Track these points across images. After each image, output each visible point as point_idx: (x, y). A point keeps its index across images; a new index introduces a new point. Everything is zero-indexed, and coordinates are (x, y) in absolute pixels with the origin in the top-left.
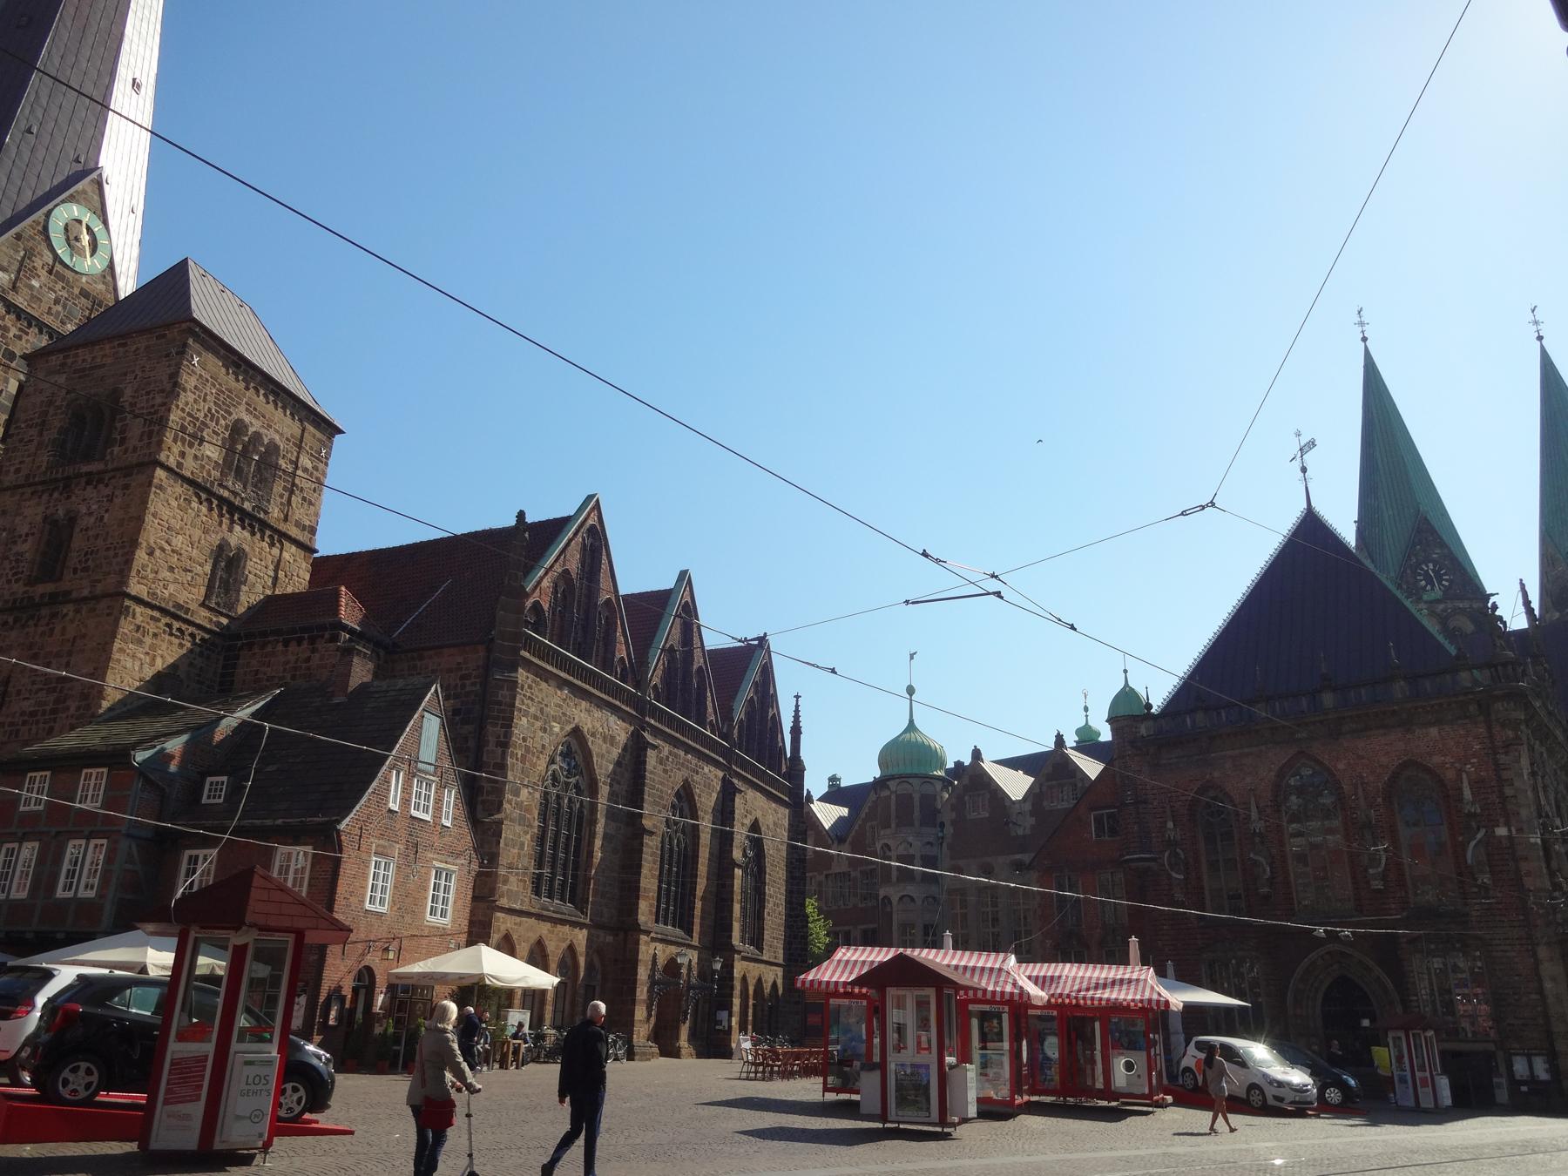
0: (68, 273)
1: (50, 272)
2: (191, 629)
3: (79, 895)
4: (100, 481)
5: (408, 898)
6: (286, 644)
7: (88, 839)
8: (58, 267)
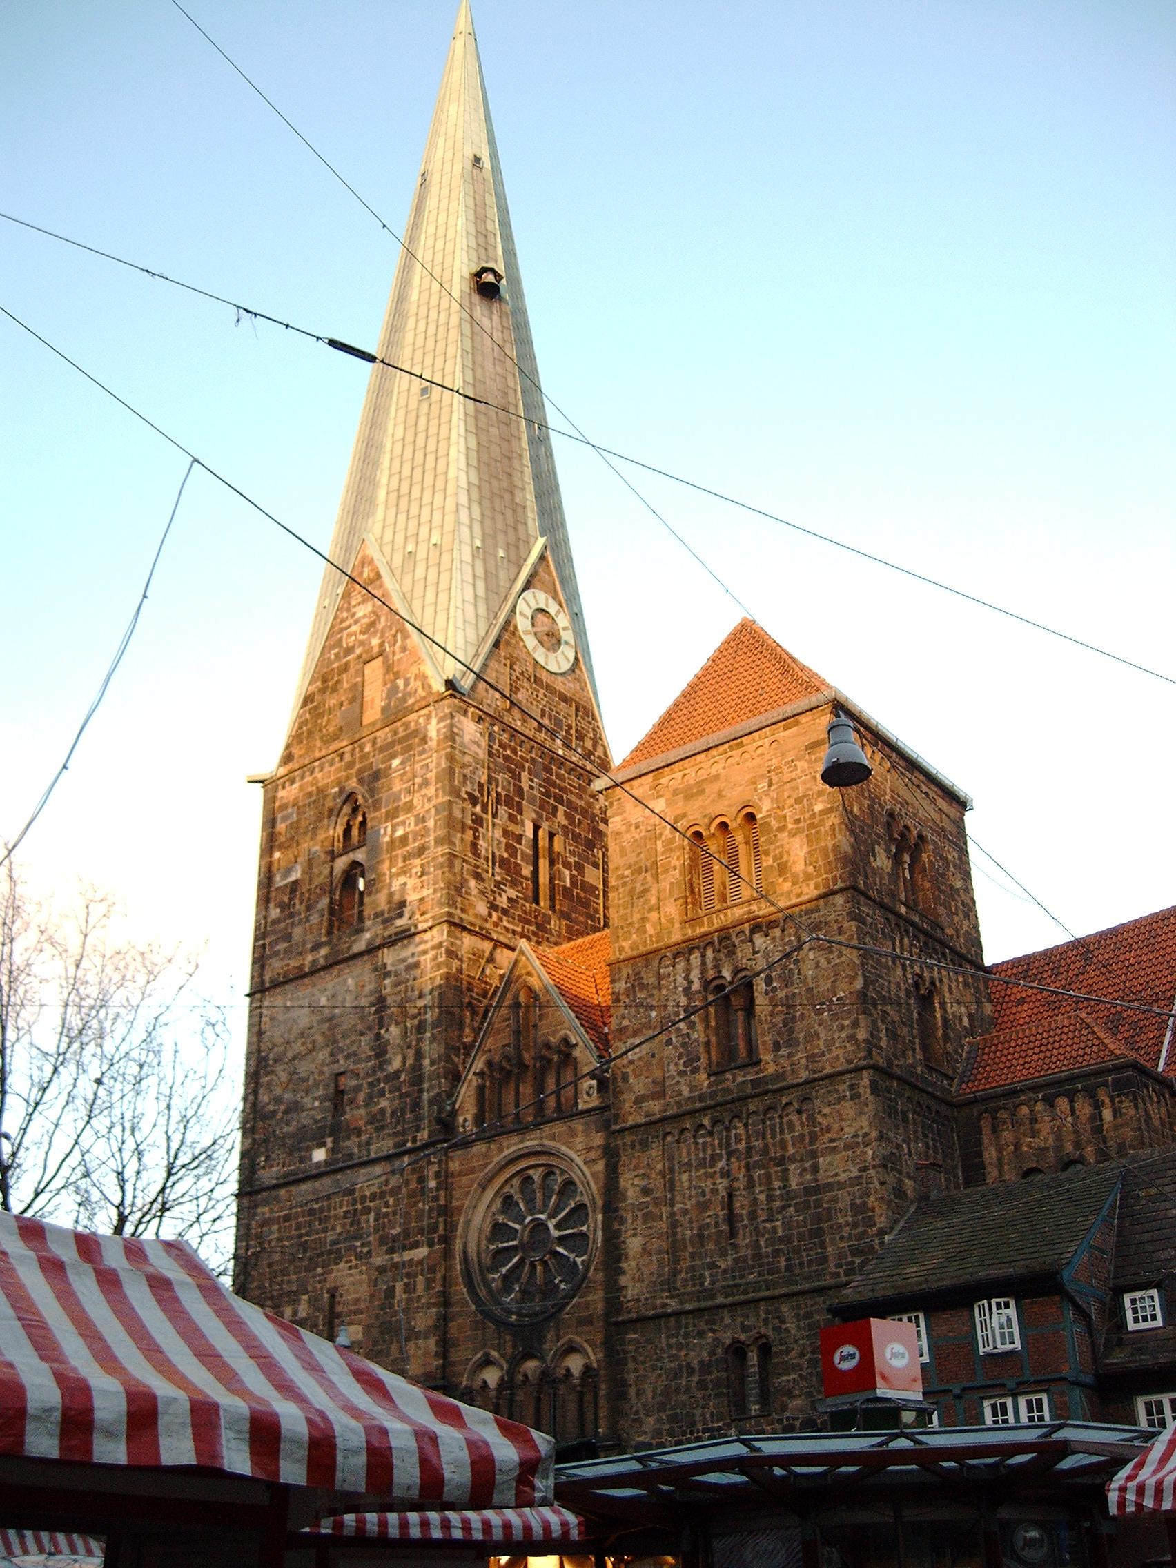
0: (544, 676)
1: (529, 680)
7: (1015, 1396)
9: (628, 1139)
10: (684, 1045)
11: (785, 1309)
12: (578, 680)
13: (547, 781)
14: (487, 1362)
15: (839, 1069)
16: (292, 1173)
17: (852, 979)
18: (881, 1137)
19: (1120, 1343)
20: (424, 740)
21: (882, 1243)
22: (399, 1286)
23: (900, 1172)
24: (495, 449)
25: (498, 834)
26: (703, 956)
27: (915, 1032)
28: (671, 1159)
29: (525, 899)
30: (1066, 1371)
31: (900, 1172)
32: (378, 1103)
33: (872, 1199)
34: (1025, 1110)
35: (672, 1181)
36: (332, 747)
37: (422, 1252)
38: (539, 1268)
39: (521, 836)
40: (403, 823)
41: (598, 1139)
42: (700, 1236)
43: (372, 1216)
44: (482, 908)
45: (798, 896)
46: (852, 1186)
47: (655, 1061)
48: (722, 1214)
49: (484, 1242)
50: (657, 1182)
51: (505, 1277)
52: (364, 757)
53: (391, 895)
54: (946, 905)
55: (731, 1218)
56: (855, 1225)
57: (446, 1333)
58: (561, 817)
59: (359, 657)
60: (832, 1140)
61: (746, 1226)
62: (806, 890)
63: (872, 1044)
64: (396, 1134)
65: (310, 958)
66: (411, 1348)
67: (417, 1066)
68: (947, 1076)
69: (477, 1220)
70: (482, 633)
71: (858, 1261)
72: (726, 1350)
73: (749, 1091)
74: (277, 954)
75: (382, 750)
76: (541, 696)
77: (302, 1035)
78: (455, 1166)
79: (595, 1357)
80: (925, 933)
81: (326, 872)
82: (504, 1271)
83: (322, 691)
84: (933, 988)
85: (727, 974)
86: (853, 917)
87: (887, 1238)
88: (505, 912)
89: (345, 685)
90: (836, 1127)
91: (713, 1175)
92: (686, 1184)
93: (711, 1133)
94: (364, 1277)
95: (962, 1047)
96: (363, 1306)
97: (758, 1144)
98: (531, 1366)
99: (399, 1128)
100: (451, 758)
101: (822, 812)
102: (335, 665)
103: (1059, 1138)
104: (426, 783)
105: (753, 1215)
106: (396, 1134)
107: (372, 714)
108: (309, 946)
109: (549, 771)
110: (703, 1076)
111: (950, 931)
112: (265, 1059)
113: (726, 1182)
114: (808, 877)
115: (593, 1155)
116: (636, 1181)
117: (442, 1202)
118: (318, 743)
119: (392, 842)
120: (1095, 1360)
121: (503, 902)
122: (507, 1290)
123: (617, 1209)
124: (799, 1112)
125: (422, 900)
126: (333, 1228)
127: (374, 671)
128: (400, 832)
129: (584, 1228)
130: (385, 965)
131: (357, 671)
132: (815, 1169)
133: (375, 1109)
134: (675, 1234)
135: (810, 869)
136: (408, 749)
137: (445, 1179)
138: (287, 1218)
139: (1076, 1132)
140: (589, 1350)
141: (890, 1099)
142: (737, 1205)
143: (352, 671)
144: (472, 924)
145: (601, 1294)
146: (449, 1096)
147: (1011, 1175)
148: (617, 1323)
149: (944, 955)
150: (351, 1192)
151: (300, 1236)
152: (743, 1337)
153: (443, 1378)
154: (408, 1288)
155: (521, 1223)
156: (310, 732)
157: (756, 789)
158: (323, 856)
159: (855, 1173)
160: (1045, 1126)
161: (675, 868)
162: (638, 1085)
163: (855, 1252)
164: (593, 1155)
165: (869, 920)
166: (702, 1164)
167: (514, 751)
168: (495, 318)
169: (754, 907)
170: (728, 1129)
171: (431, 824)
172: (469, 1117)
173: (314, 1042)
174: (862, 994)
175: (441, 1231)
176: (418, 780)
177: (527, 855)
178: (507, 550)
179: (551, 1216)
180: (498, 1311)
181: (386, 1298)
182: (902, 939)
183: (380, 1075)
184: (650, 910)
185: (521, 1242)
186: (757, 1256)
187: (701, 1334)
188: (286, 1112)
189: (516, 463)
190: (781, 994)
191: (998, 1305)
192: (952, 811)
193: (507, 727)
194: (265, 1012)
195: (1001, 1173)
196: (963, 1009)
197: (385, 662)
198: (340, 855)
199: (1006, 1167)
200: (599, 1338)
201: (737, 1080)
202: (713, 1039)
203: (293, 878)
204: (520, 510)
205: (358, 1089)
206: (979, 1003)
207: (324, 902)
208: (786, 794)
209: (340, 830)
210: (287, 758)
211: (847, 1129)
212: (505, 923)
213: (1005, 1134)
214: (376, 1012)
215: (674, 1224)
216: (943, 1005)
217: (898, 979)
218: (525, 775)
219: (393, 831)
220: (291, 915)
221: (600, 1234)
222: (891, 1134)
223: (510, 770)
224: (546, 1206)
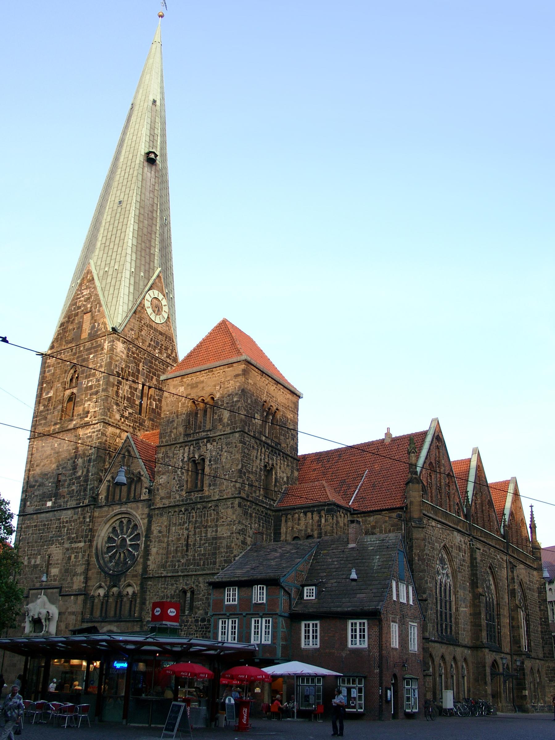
0: (153, 325)
1: (147, 326)
3: (263, 643)
4: (214, 441)
9: (157, 512)
10: (179, 480)
11: (201, 579)
12: (168, 326)
13: (150, 367)
14: (100, 587)
15: (229, 497)
16: (38, 509)
17: (237, 465)
18: (239, 522)
19: (301, 603)
21: (234, 560)
22: (73, 556)
23: (246, 535)
24: (145, 230)
25: (127, 388)
26: (189, 448)
27: (261, 484)
28: (170, 521)
29: (136, 413)
30: (278, 612)
31: (246, 535)
32: (72, 487)
33: (233, 544)
34: (297, 515)
35: (169, 529)
36: (70, 346)
37: (82, 545)
38: (122, 555)
39: (137, 388)
40: (91, 380)
41: (146, 511)
42: (176, 550)
43: (66, 529)
44: (118, 417)
45: (224, 431)
46: (227, 539)
47: (168, 485)
48: (185, 543)
49: (104, 543)
50: (164, 529)
51: (110, 556)
52: (80, 352)
53: (84, 408)
54: (284, 435)
55: (187, 545)
56: (227, 553)
57: (87, 575)
58: (154, 381)
59: (83, 311)
60: (223, 522)
61: (191, 548)
62: (227, 429)
63: (240, 490)
64: (77, 500)
65: (53, 428)
66: (75, 578)
67: (87, 475)
68: (273, 500)
69: (102, 534)
70: (130, 308)
71: (226, 565)
72: (180, 591)
73: (198, 500)
74: (41, 424)
75: (87, 350)
76: (151, 332)
77: (47, 457)
78: (96, 514)
79: (137, 589)
80: (272, 447)
81: (62, 395)
82: (110, 554)
83: (68, 322)
85: (197, 456)
86: (241, 442)
87: (237, 558)
88: (127, 418)
89: (76, 322)
90: (225, 517)
91: (183, 529)
92: (174, 531)
93: (184, 514)
96: (59, 562)
97: (199, 520)
98: (115, 590)
99: (78, 498)
100: (111, 358)
101: (236, 401)
103: (306, 527)
104: (101, 366)
105: (194, 545)
106: (77, 500)
107: (85, 335)
108: (53, 423)
110: (184, 493)
111: (283, 445)
112: (33, 464)
113: (187, 532)
114: (228, 425)
115: (144, 516)
117: (91, 527)
118: (64, 343)
119: (87, 387)
120: (290, 608)
121: (126, 414)
122: (111, 562)
123: (150, 537)
124: (214, 510)
125: (95, 412)
126: (52, 532)
127: (87, 317)
128: (90, 384)
129: (139, 542)
131: (81, 317)
132: (217, 531)
134: (168, 548)
135: (229, 422)
136: (96, 352)
137: (92, 518)
138: (36, 526)
139: (312, 525)
140: (135, 586)
141: (246, 509)
142: (189, 540)
143: (79, 316)
144: (113, 423)
145: (141, 567)
146: (97, 488)
147: (289, 538)
148: (145, 578)
149: (279, 454)
150: (59, 519)
151: (40, 533)
152: (185, 587)
153: (85, 591)
154: (76, 557)
155: (118, 538)
156: (61, 338)
157: (215, 389)
158: (61, 388)
159: (229, 534)
160: (302, 522)
162: (162, 493)
163: (225, 561)
164: (144, 516)
165: (248, 443)
166: (180, 524)
167: (138, 355)
168: (153, 172)
169: (209, 433)
170: (190, 513)
171: (101, 382)
172: (103, 497)
173: (51, 461)
174: (240, 471)
175: (89, 538)
176: (99, 365)
177: (138, 396)
178: (145, 273)
179: (128, 536)
180: (106, 569)
181: (68, 560)
182: (261, 449)
183: (73, 476)
185: (117, 545)
186: (194, 559)
187: (172, 585)
188: (39, 486)
189: (153, 236)
190: (214, 466)
191: (260, 587)
192: (294, 398)
193: (135, 346)
194: (35, 446)
195: (286, 537)
196: (285, 475)
197: (92, 315)
198: (68, 389)
199: (288, 535)
200: (139, 582)
201: (195, 496)
202: (189, 480)
203: (49, 395)
204: (152, 256)
205: (65, 481)
206: (292, 472)
207: (61, 406)
209: (69, 379)
210: (52, 347)
213: (289, 523)
214: (75, 452)
215: (168, 545)
216: (276, 474)
217: (257, 464)
218: (141, 364)
219: (88, 383)
220: (48, 410)
221: (143, 545)
222: (244, 522)
223: (135, 363)
224: (127, 532)
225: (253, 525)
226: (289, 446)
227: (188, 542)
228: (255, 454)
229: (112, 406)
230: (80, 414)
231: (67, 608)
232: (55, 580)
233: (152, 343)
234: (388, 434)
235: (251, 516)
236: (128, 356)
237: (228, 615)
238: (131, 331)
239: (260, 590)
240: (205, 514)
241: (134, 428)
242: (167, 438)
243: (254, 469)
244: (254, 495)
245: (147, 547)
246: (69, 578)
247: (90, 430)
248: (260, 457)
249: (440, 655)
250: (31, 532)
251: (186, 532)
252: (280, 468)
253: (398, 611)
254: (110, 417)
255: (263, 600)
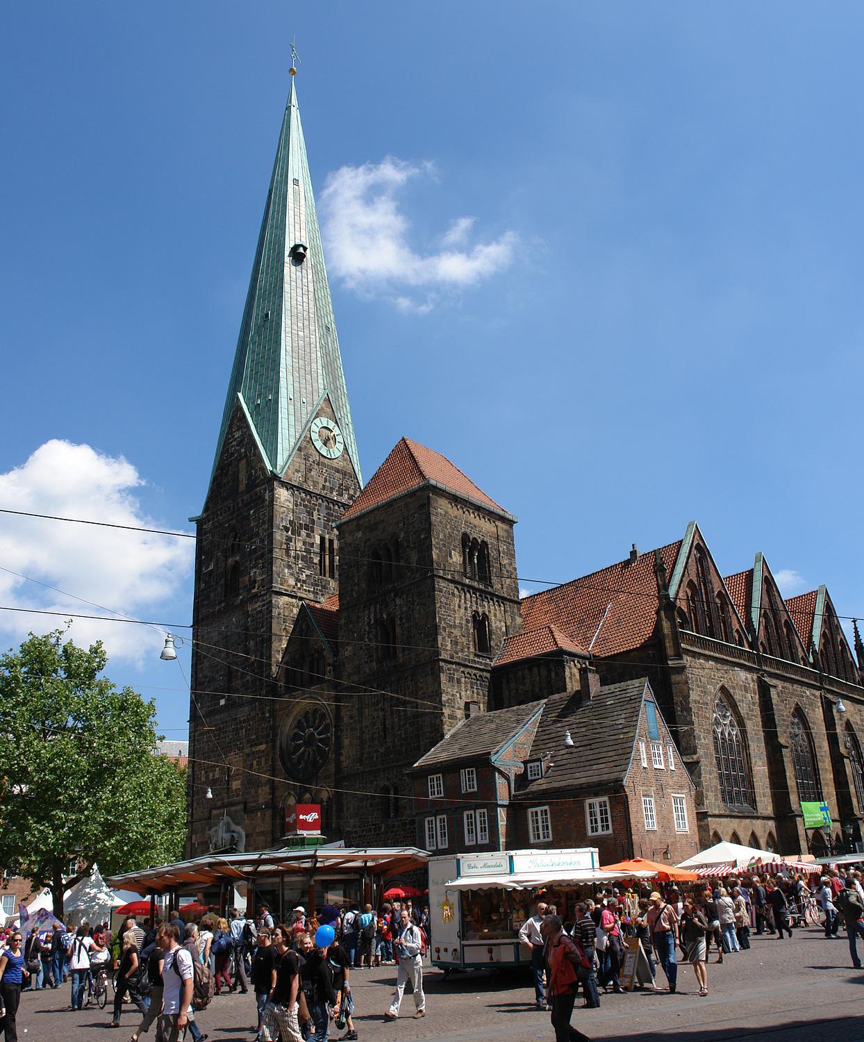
0: (326, 461)
1: (318, 464)
2: (474, 671)
5: (665, 821)
6: (530, 670)
8: (322, 459)
10: (367, 649)
20: (264, 500)
22: (255, 762)
25: (299, 545)
26: (375, 607)
29: (316, 574)
31: (453, 707)
34: (520, 673)
37: (263, 747)
39: (313, 543)
40: (255, 542)
44: (292, 582)
48: (381, 727)
53: (250, 577)
55: (385, 729)
56: (431, 733)
59: (236, 457)
62: (417, 577)
65: (218, 608)
74: (204, 606)
81: (224, 565)
84: (485, 617)
85: (384, 616)
88: (304, 582)
90: (425, 688)
94: (241, 758)
95: (501, 642)
102: (226, 462)
107: (242, 488)
108: (217, 602)
109: (330, 509)
110: (374, 664)
113: (383, 713)
116: (348, 713)
118: (220, 502)
121: (303, 577)
124: (412, 681)
128: (253, 547)
130: (248, 611)
133: (244, 681)
144: (285, 590)
145: (334, 765)
152: (387, 783)
158: (222, 558)
161: (365, 565)
176: (261, 521)
182: (465, 594)
183: (247, 664)
184: (355, 586)
187: (372, 782)
190: (406, 626)
191: (468, 771)
192: (505, 527)
194: (199, 634)
197: (247, 460)
206: (513, 619)
208: (410, 530)
210: (206, 509)
211: (429, 689)
212: (305, 588)
215: (362, 733)
218: (315, 513)
219: (251, 547)
220: (210, 587)
221: (333, 737)
224: (314, 722)
225: (463, 693)
226: (505, 586)
227: (385, 725)
228: (457, 602)
229: (283, 570)
230: (247, 585)
231: (255, 828)
232: (238, 795)
233: (327, 484)
234: (633, 553)
235: (459, 681)
236: (296, 505)
237: (434, 812)
238: (296, 474)
239: (469, 774)
240: (401, 687)
241: (315, 593)
242: (348, 598)
243: (457, 621)
244: (460, 654)
245: (338, 738)
246: (253, 791)
247: (259, 604)
248: (464, 605)
249: (731, 833)
250: (205, 740)
251: (381, 714)
252: (495, 616)
253: (653, 780)
254: (281, 584)
255: (473, 788)
